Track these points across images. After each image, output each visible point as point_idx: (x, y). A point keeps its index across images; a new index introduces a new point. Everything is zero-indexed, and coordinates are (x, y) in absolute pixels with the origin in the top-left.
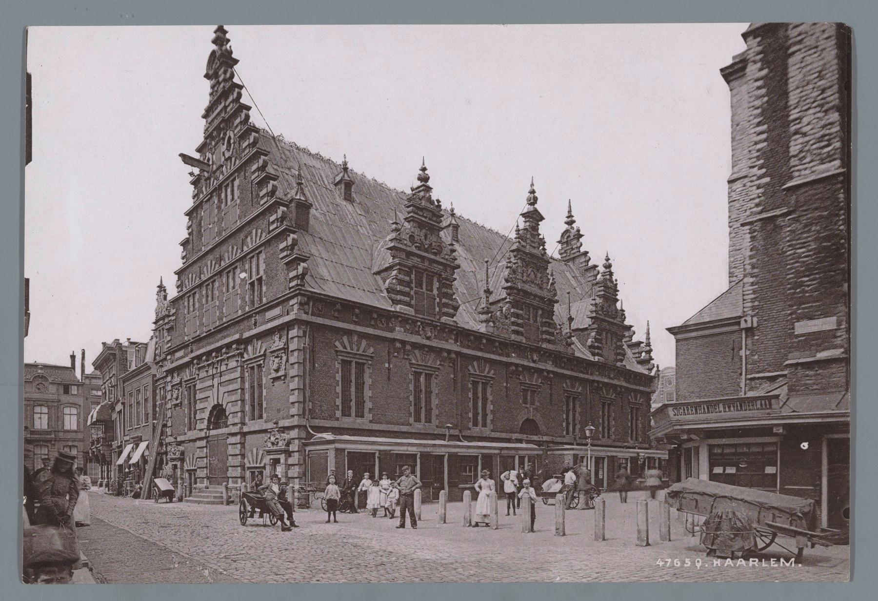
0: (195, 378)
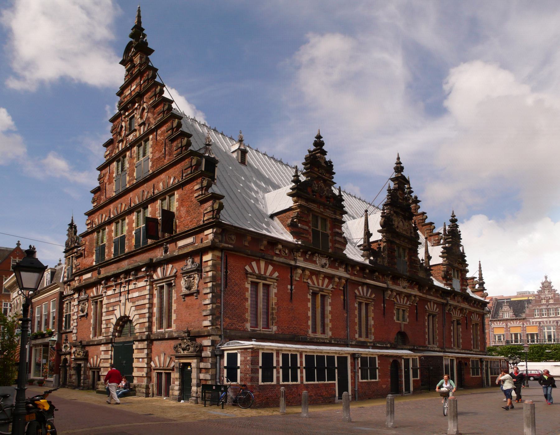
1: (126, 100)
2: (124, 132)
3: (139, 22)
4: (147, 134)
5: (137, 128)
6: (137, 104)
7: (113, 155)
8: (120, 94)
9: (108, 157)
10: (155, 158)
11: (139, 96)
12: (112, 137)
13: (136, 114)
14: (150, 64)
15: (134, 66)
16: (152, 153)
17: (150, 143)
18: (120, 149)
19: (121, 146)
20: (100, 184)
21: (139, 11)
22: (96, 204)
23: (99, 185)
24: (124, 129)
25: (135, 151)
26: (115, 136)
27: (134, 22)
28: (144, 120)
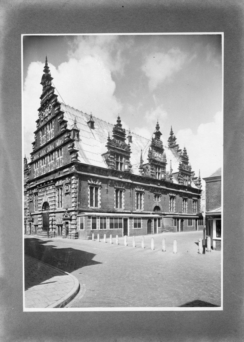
7: (40, 127)
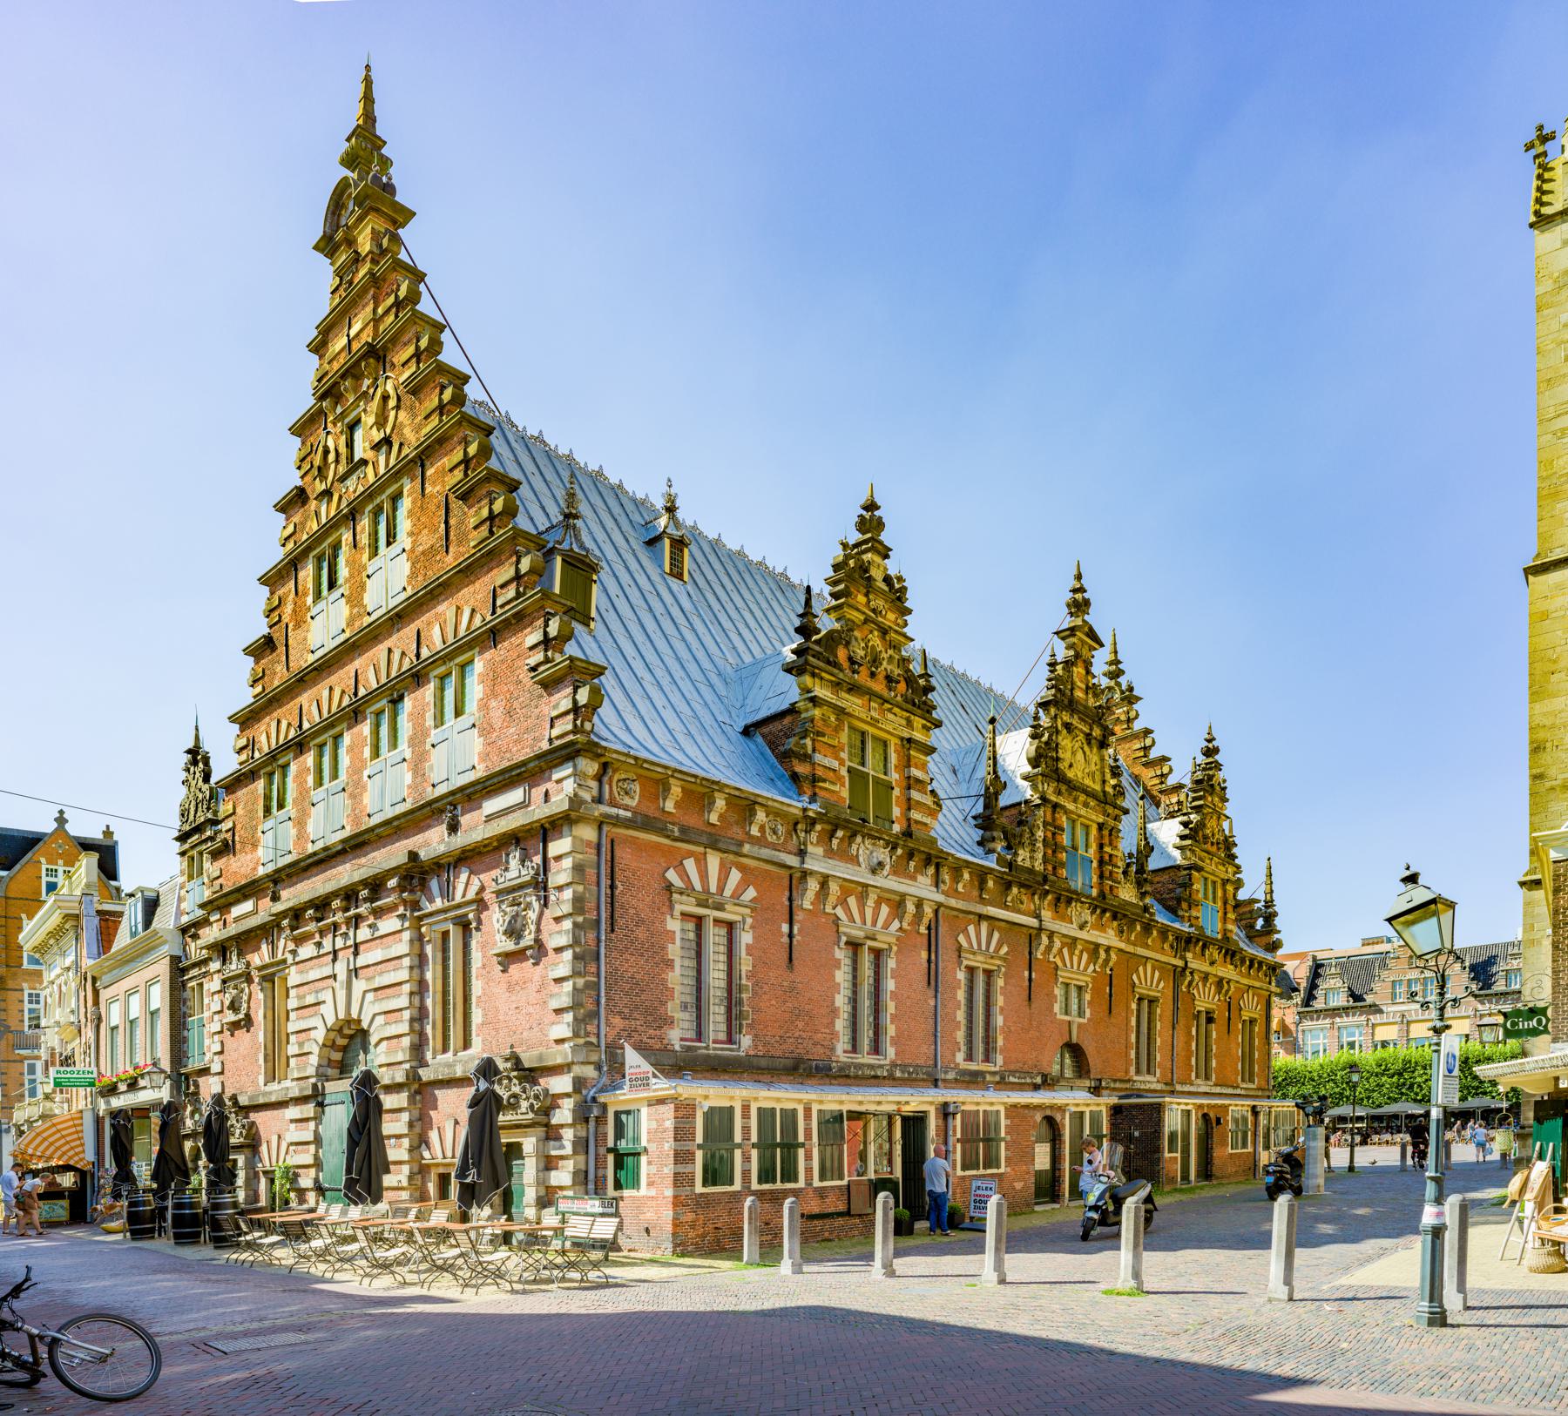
0: (284, 961)
1: (336, 366)
2: (333, 466)
3: (369, 117)
4: (395, 475)
5: (369, 455)
6: (367, 382)
7: (305, 537)
8: (318, 347)
9: (290, 545)
10: (421, 549)
11: (376, 355)
12: (299, 483)
13: (365, 410)
14: (403, 256)
15: (357, 259)
16: (411, 534)
17: (406, 504)
18: (324, 521)
19: (327, 511)
20: (271, 627)
21: (368, 81)
22: (259, 689)
23: (268, 630)
24: (331, 457)
25: (364, 529)
26: (308, 478)
27: (352, 116)
28: (388, 431)
